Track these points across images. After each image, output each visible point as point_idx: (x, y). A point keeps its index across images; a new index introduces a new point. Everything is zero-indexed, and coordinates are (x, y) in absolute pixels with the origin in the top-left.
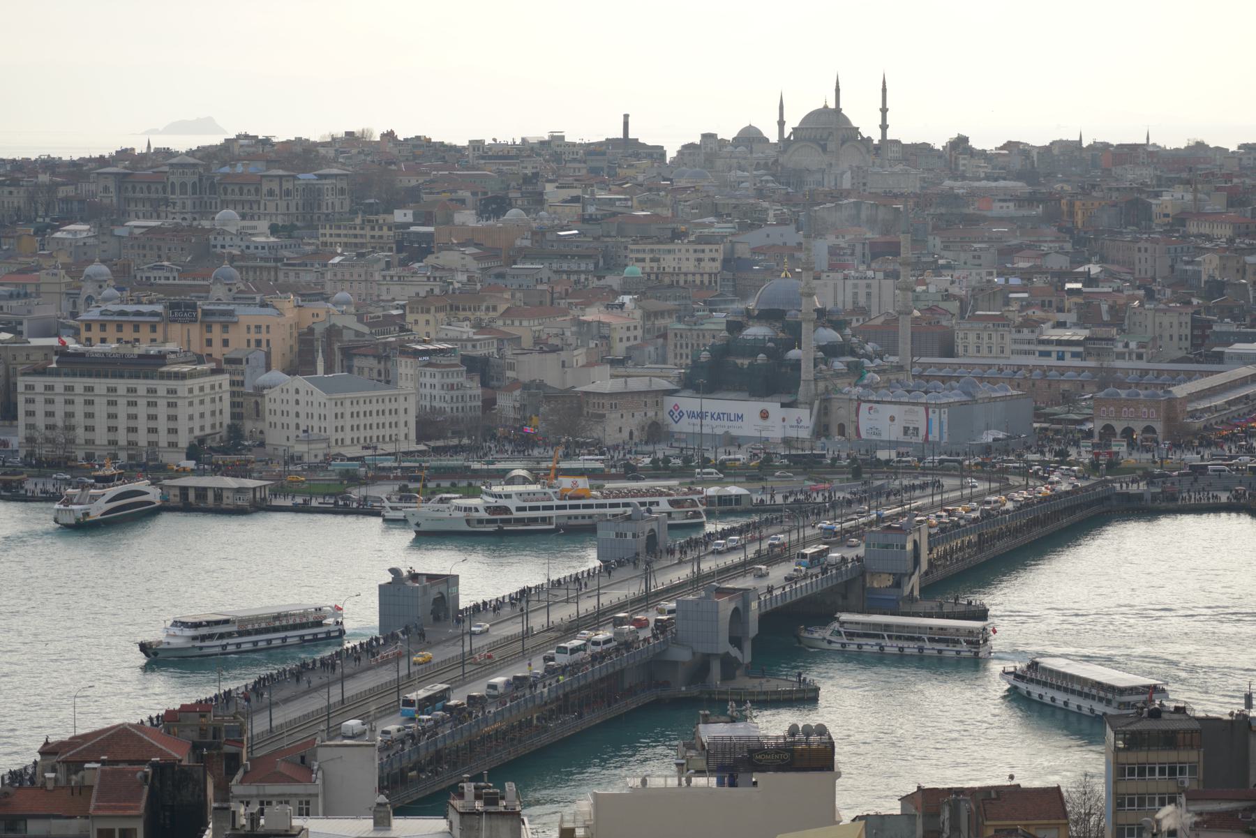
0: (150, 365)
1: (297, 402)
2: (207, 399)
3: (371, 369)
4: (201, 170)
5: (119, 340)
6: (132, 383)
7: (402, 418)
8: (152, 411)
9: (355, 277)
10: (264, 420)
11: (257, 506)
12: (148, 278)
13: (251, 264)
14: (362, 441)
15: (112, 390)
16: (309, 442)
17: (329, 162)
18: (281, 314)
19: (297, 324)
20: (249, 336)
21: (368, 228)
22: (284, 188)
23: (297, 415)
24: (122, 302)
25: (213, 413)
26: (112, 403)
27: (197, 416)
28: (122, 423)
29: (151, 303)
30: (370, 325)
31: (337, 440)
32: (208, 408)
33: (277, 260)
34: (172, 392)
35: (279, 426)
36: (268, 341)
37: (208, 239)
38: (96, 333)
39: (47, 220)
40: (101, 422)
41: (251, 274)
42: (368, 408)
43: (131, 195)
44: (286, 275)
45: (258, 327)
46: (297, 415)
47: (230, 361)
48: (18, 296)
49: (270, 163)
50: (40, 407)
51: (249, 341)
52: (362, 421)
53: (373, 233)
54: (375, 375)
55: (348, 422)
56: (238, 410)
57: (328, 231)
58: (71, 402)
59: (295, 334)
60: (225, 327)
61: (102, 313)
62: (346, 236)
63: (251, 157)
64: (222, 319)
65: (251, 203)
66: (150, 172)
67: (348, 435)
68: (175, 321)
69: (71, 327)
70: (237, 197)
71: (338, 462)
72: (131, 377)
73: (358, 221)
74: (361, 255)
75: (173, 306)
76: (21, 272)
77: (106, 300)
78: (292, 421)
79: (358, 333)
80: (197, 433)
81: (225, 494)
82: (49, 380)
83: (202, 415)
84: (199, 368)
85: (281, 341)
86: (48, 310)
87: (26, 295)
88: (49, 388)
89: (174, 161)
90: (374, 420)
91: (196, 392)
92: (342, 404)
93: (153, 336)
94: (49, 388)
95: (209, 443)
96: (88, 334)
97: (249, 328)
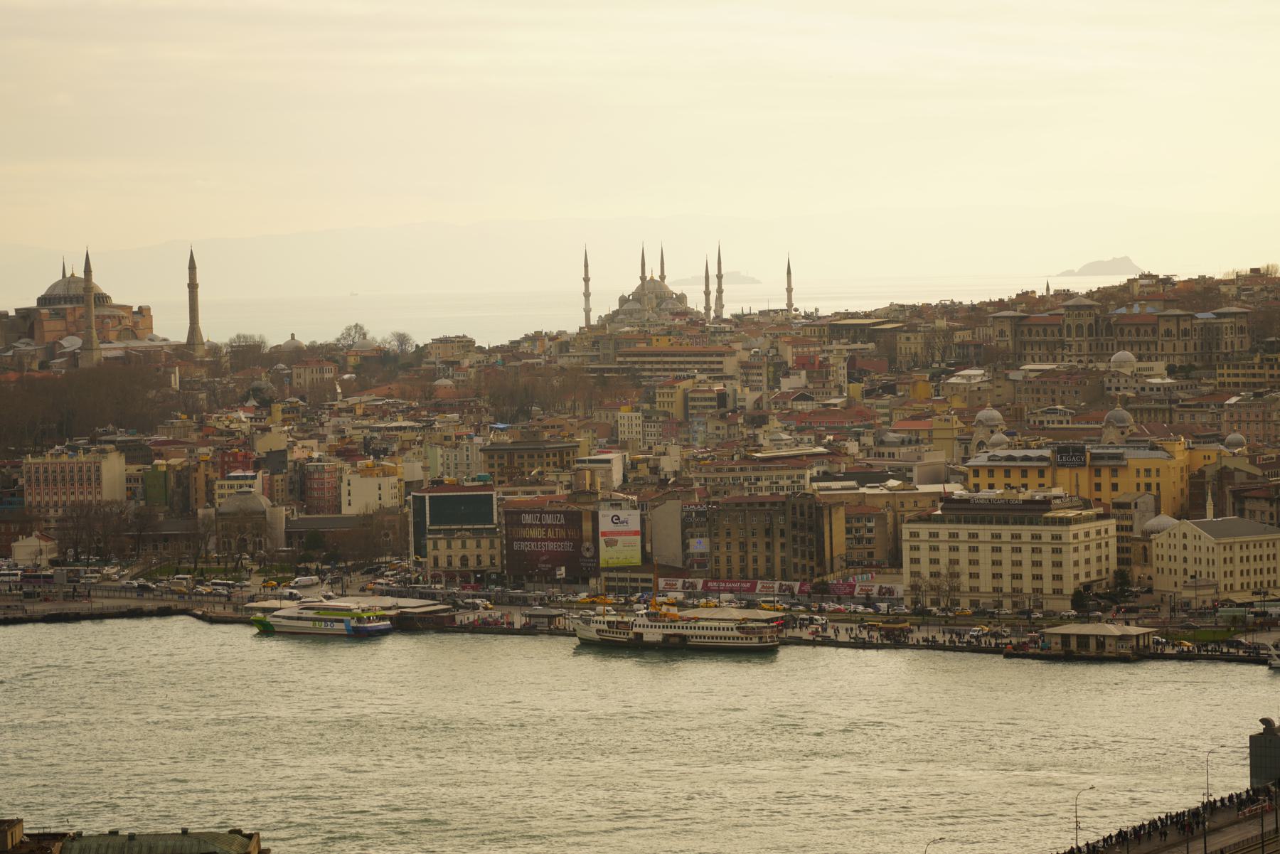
0: (1034, 511)
1: (1185, 547)
2: (1093, 545)
3: (1263, 512)
4: (1098, 312)
5: (1008, 486)
6: (1017, 529)
8: (1037, 557)
9: (1253, 418)
10: (1151, 565)
11: (1139, 654)
12: (1041, 422)
13: (1145, 405)
14: (1252, 586)
15: (996, 536)
16: (1196, 587)
17: (1227, 300)
18: (1172, 457)
19: (1188, 467)
20: (1138, 480)
21: (1267, 367)
22: (1182, 327)
23: (1185, 560)
24: (1010, 447)
25: (1099, 559)
26: (996, 550)
27: (1082, 562)
28: (1007, 569)
29: (1039, 447)
30: (1262, 467)
31: (1226, 586)
32: (1093, 554)
33: (1171, 401)
34: (1057, 537)
35: (1166, 572)
36: (1158, 485)
37: (1102, 382)
38: (983, 479)
39: (943, 365)
40: (985, 569)
41: (1146, 416)
42: (1258, 552)
43: (1027, 338)
44: (1182, 416)
45: (1148, 471)
46: (1185, 560)
47: (1118, 506)
48: (910, 442)
49: (1168, 302)
50: (924, 555)
51: (1138, 485)
52: (1252, 565)
53: (1271, 372)
54: (1267, 518)
55: (1238, 567)
56: (1126, 555)
57: (1225, 371)
58: (955, 549)
59: (1186, 477)
60: (1114, 471)
61: (990, 459)
62: (1244, 375)
63: (1150, 298)
64: (1112, 463)
65: (1148, 343)
66: (1046, 315)
67: (1238, 581)
68: (1063, 466)
69: (961, 473)
70: (1135, 338)
71: (1226, 608)
72: (1015, 523)
73: (1257, 360)
74: (1257, 395)
75: (1061, 451)
76: (914, 418)
77: (995, 445)
78: (1179, 565)
79: (1250, 476)
80: (1083, 579)
81: (1107, 642)
82: (934, 527)
83: (1088, 561)
84: (1084, 513)
85: (1172, 484)
86: (936, 457)
87: (917, 441)
88: (934, 535)
89: (1070, 303)
91: (1081, 537)
93: (1042, 481)
94: (934, 535)
95: (1095, 589)
96: (976, 480)
97: (1138, 471)
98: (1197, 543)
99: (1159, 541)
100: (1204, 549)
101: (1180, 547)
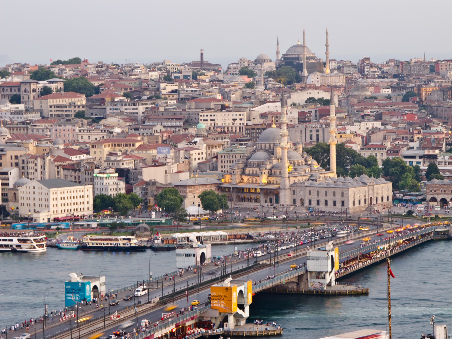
1: (34, 193)
7: (86, 199)
10: (18, 202)
20: (11, 161)
21: (73, 107)
22: (32, 88)
23: (34, 199)
35: (25, 205)
46: (34, 199)
51: (12, 164)
52: (66, 201)
53: (75, 109)
55: (60, 202)
56: (6, 197)
62: (61, 111)
90: (73, 201)
92: (56, 193)
98: (40, 191)
99: (22, 190)
100: (43, 194)
101: (32, 193)
